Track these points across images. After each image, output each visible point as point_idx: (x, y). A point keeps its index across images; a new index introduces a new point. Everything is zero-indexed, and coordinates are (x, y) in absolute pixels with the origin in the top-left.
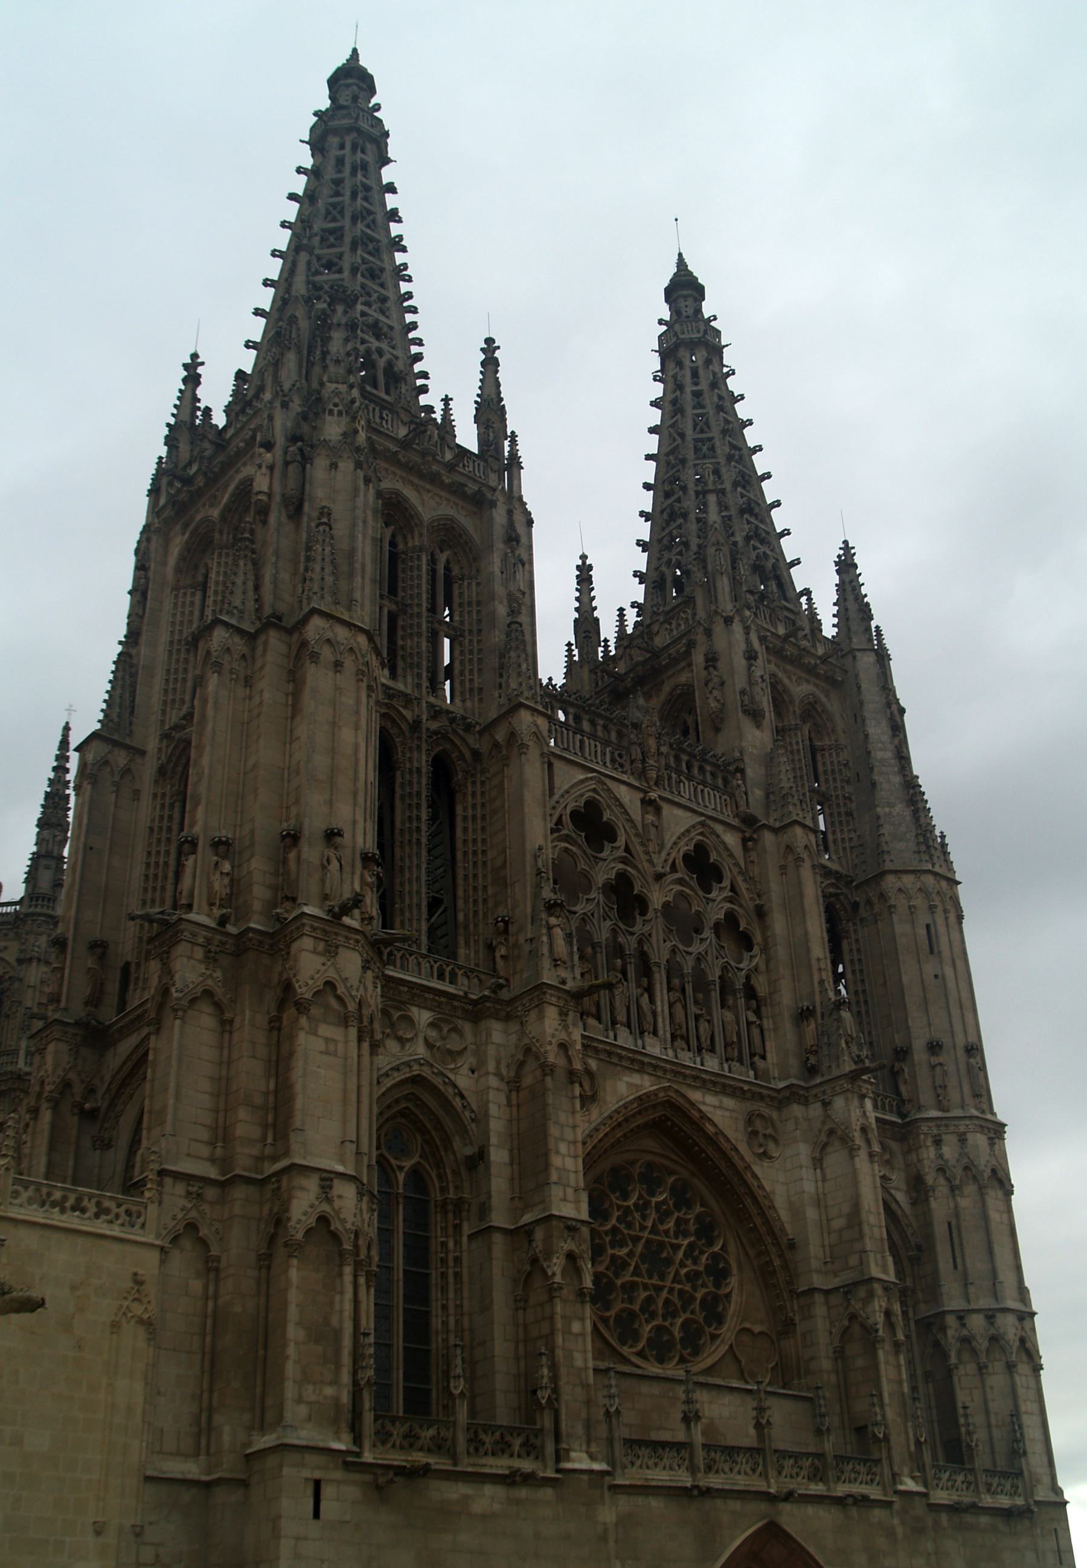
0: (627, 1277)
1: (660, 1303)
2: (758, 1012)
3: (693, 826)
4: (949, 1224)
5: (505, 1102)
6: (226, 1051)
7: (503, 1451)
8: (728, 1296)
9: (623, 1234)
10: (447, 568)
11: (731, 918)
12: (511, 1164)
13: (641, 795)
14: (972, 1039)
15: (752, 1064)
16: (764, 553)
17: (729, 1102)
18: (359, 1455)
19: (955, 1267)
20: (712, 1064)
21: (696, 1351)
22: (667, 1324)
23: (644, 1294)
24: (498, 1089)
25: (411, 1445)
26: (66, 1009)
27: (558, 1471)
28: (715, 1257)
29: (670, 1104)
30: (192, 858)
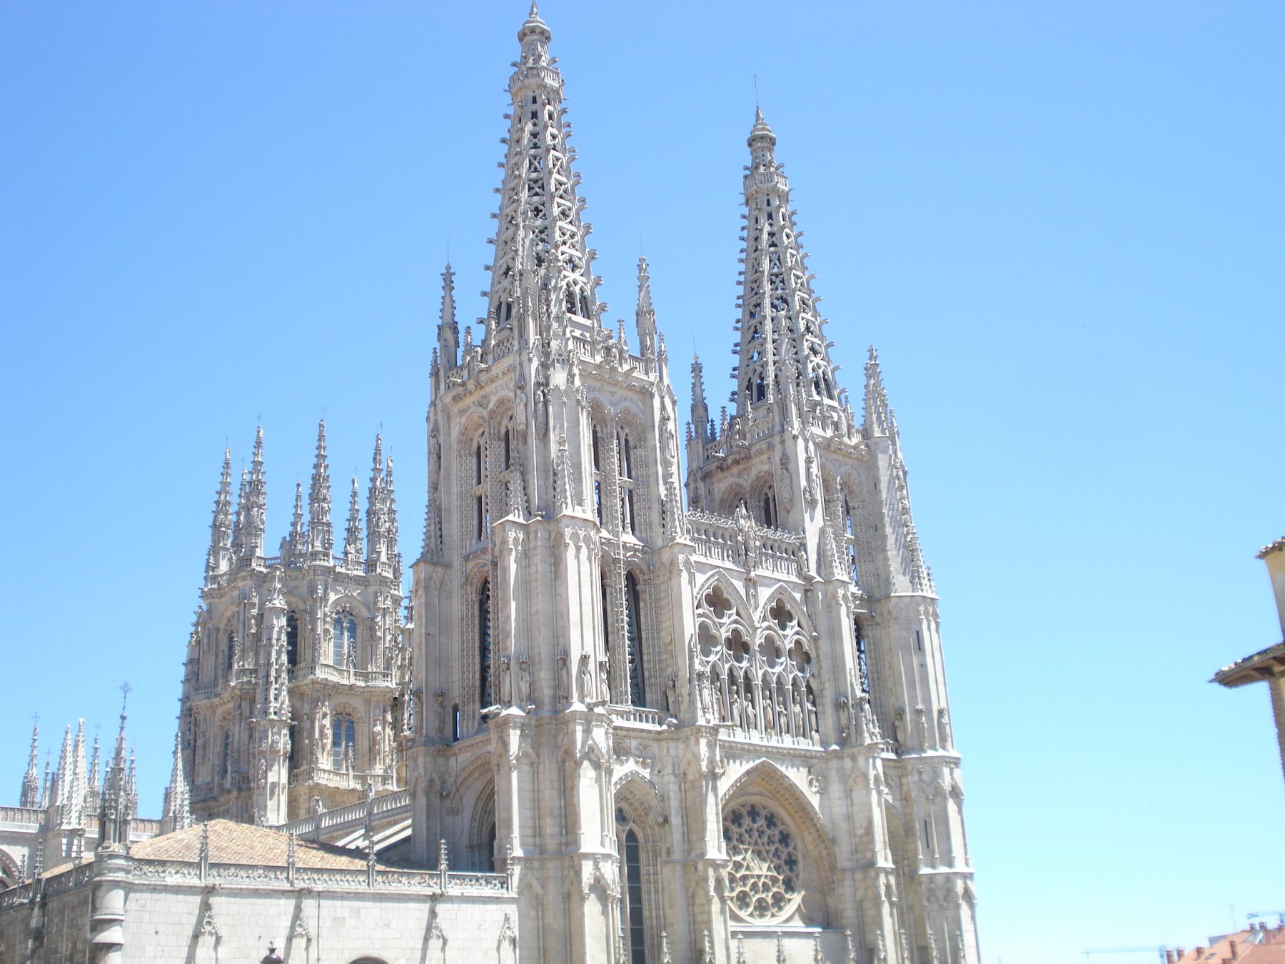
1: (760, 884)
2: (814, 704)
4: (925, 821)
6: (536, 785)
8: (797, 876)
10: (627, 441)
11: (798, 643)
12: (683, 825)
14: (943, 705)
16: (817, 364)
19: (928, 847)
21: (780, 909)
23: (752, 881)
24: (674, 783)
26: (427, 736)
30: (509, 672)
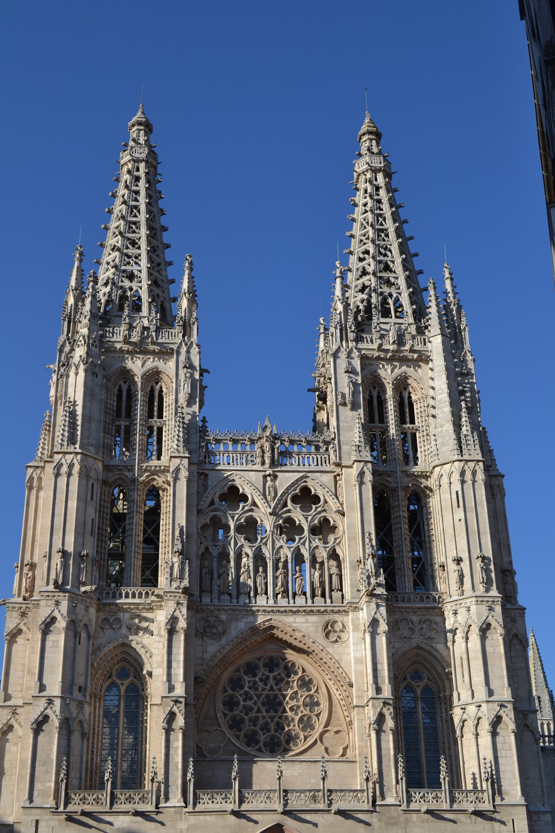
0: (253, 714)
3: (297, 480)
5: (162, 647)
7: (130, 802)
8: (318, 715)
9: (251, 694)
13: (264, 473)
15: (331, 597)
17: (313, 619)
18: (57, 809)
20: (300, 601)
22: (277, 734)
25: (84, 803)
27: (156, 808)
28: (311, 696)
29: (272, 627)
